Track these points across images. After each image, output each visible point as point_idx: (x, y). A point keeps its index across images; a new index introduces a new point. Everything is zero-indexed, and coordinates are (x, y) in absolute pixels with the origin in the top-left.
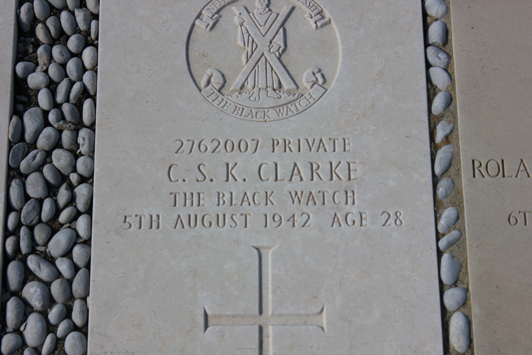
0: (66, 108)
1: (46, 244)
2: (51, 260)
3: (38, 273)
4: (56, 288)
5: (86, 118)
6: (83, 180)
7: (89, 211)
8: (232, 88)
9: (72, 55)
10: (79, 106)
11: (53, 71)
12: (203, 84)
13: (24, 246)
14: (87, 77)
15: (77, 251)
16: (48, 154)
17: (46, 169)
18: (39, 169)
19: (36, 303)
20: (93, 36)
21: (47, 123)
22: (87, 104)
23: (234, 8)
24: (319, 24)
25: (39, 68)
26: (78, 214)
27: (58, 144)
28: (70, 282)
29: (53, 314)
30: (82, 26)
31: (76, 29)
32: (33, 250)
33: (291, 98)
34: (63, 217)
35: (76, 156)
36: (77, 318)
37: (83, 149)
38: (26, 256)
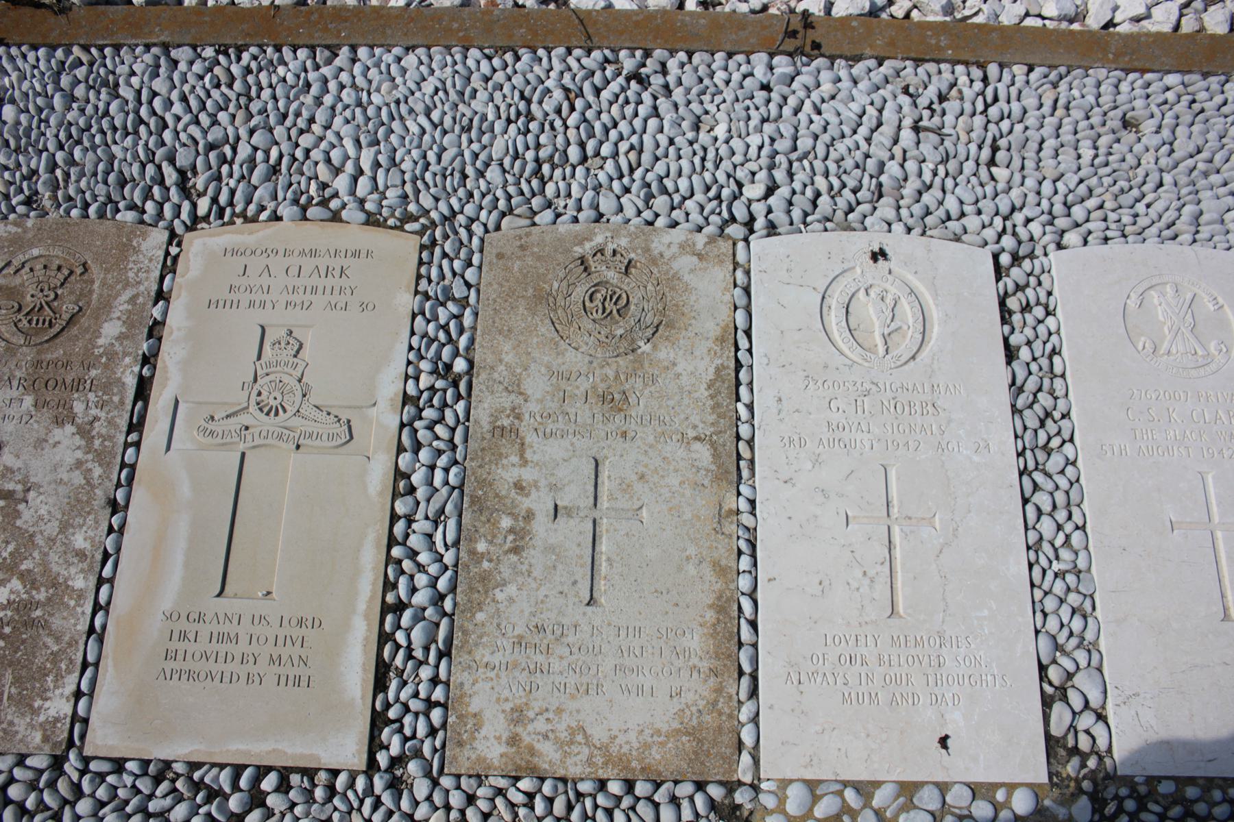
0: (1044, 362)
1: (1044, 464)
2: (1050, 476)
3: (1043, 487)
4: (1060, 498)
5: (1058, 369)
6: (1063, 417)
7: (1071, 440)
8: (1162, 352)
9: (1040, 322)
10: (1050, 358)
11: (1029, 332)
12: (1140, 348)
13: (1031, 465)
14: (1054, 338)
15: (1070, 470)
16: (1035, 395)
17: (1036, 406)
18: (1030, 406)
19: (1047, 508)
20: (1051, 308)
21: (1030, 373)
22: (1056, 359)
23: (1152, 292)
24: (1216, 307)
25: (1017, 331)
26: (1064, 442)
27: (1040, 390)
28: (1067, 493)
29: (1061, 516)
30: (1043, 300)
31: (1038, 303)
32: (1036, 469)
33: (1206, 362)
34: (1055, 442)
35: (1056, 398)
36: (1077, 518)
37: (1059, 392)
38: (1031, 472)
